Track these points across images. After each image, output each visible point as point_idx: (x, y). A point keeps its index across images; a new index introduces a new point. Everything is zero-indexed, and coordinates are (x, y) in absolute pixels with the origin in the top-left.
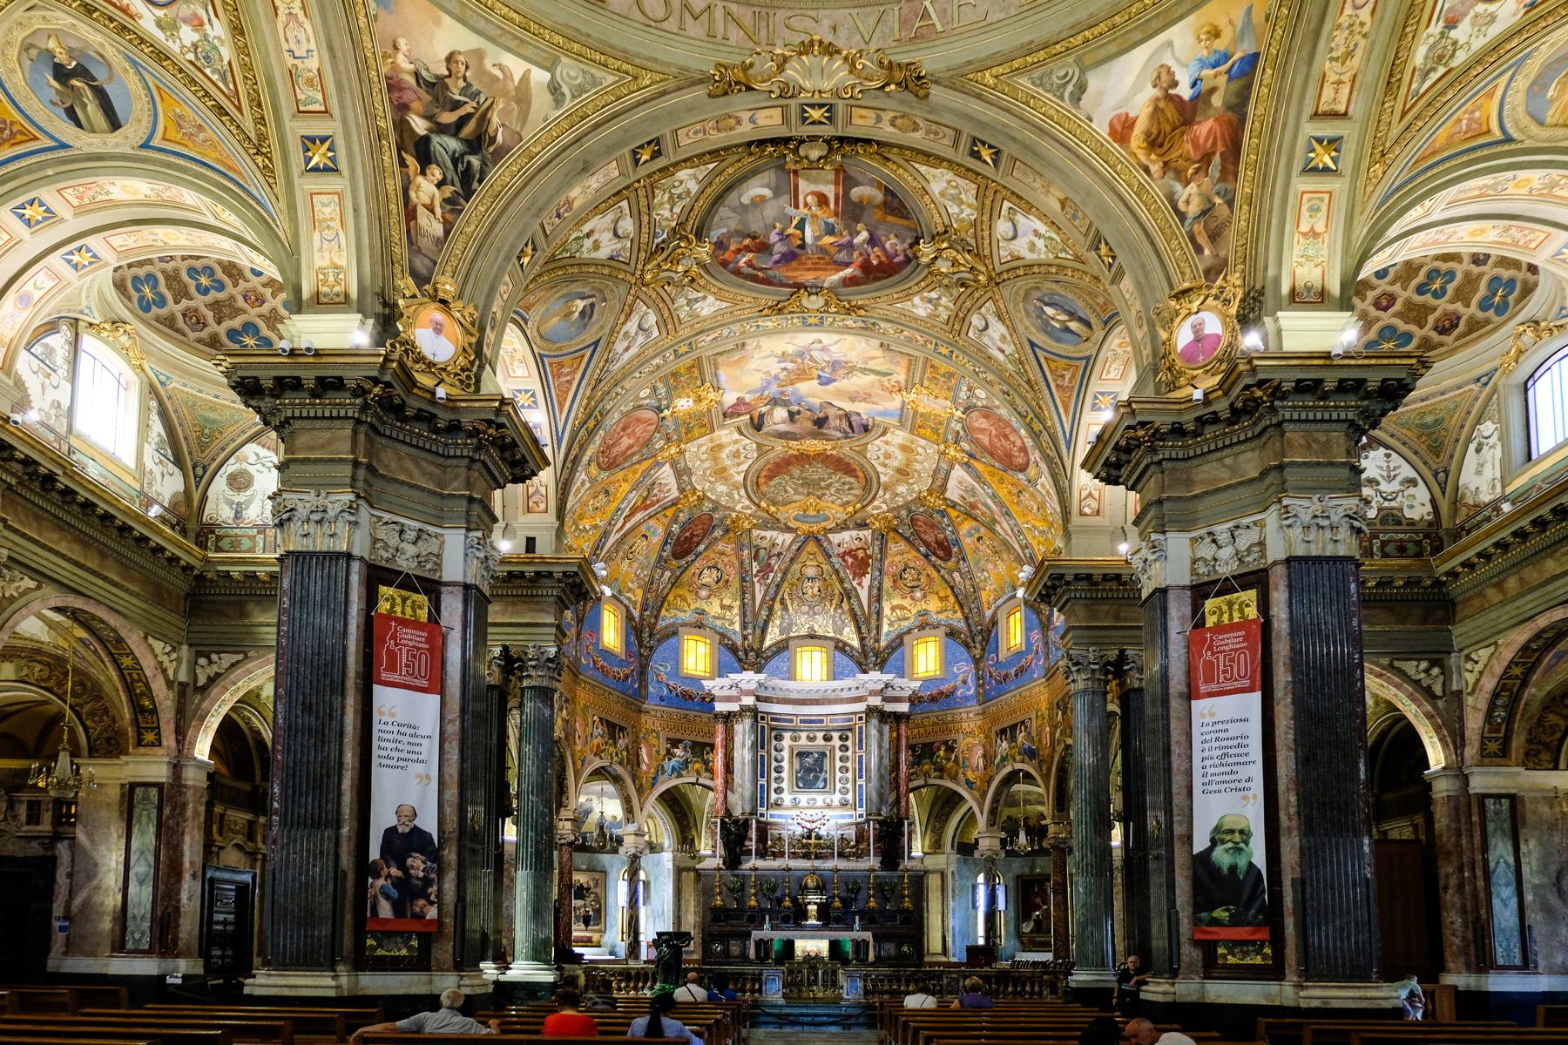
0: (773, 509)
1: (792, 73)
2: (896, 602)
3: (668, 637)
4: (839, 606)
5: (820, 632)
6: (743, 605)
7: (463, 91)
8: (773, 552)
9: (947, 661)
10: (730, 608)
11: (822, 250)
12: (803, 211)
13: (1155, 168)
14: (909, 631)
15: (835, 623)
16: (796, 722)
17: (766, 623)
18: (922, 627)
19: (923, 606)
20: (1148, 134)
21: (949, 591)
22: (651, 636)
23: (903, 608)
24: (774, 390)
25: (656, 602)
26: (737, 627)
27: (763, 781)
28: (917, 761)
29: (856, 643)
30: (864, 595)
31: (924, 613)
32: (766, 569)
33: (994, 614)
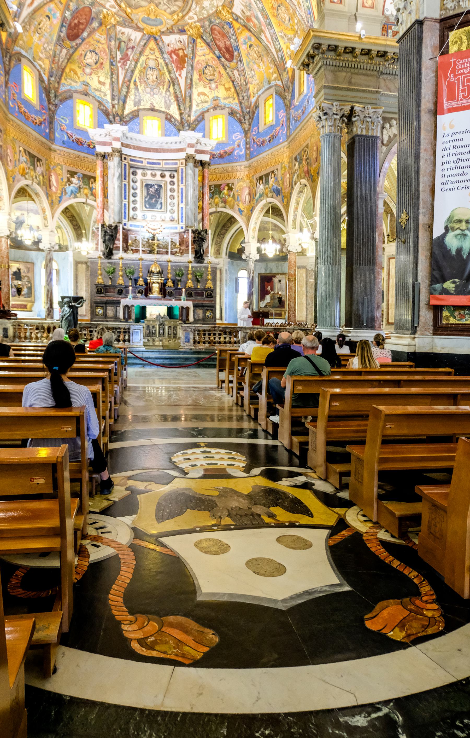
0: (129, 10)
4: (168, 90)
5: (157, 107)
6: (112, 83)
10: (104, 84)
14: (208, 111)
15: (165, 102)
17: (126, 97)
18: (215, 108)
22: (56, 96)
23: (204, 94)
26: (109, 98)
27: (125, 202)
29: (177, 117)
31: (216, 99)
32: (125, 58)
33: (257, 100)
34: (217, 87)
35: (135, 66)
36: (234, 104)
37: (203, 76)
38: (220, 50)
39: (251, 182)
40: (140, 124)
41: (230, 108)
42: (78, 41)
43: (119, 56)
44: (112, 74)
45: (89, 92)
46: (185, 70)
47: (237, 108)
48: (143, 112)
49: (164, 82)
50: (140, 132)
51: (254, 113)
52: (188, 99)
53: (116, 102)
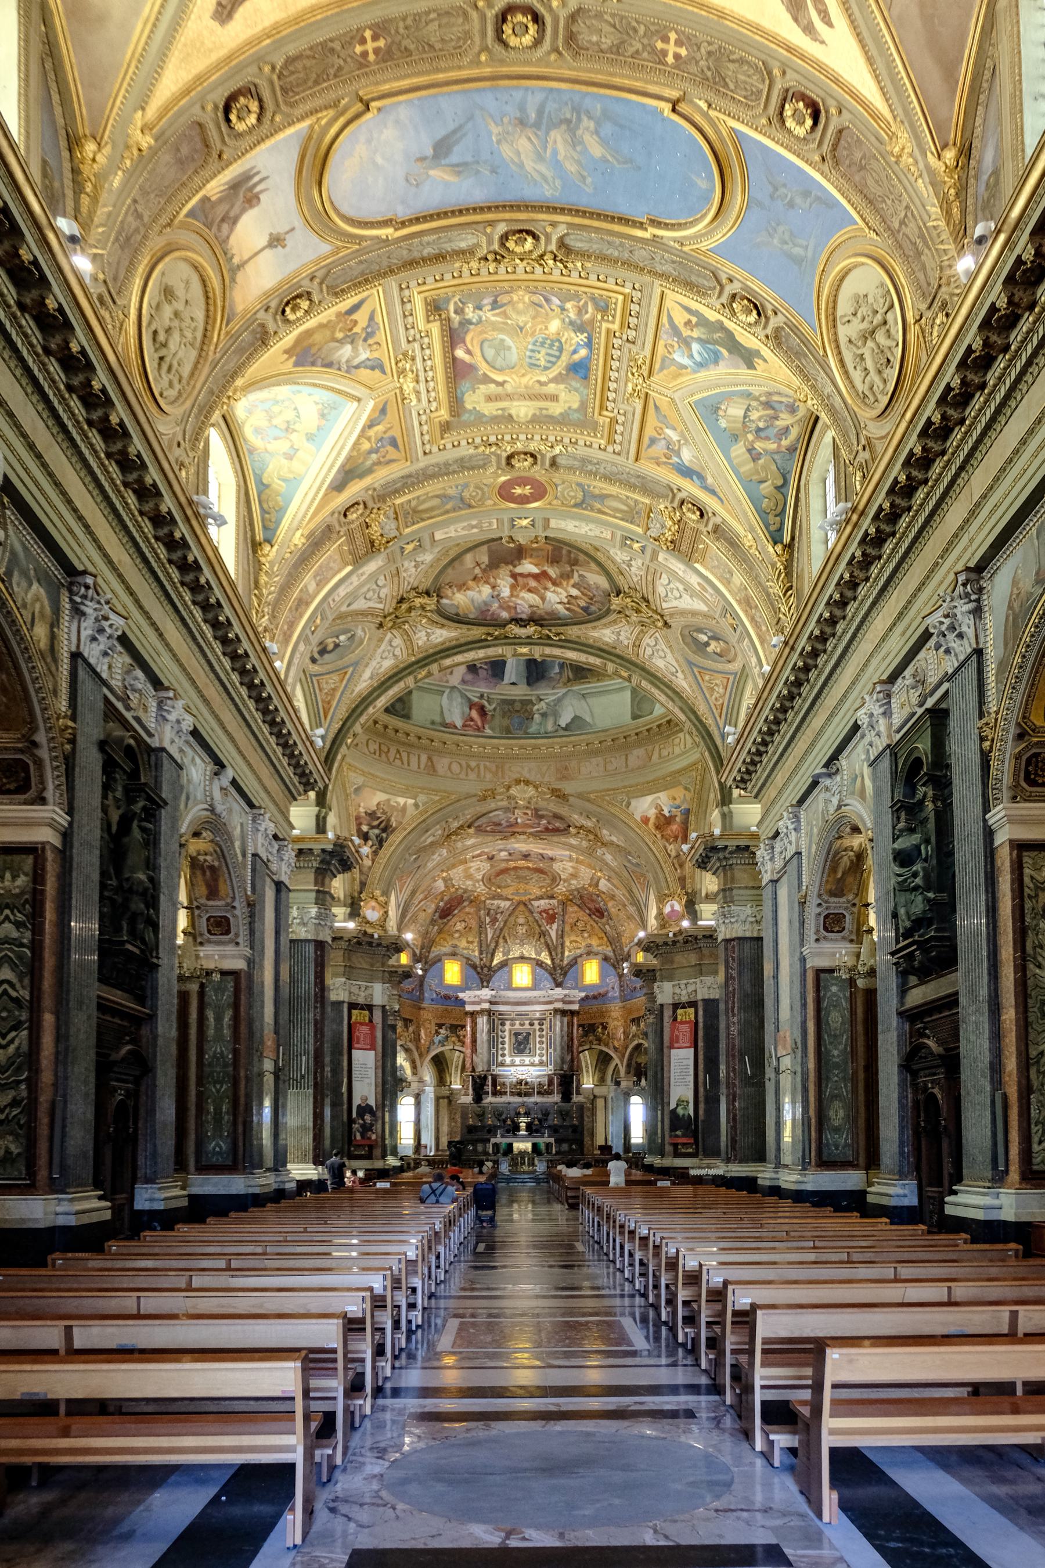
1: (513, 791)
2: (573, 938)
5: (527, 955)
8: (498, 911)
9: (603, 975)
16: (513, 1015)
17: (494, 951)
18: (588, 954)
19: (589, 941)
26: (477, 954)
28: (586, 1034)
29: (549, 962)
30: (553, 934)
31: (589, 946)
32: (494, 920)
40: (510, 973)
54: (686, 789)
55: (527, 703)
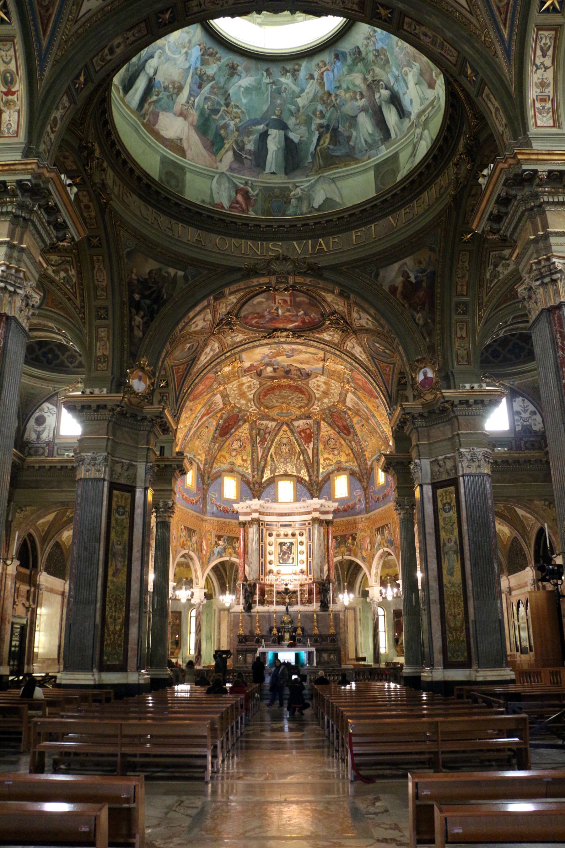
3: (217, 478)
4: (298, 458)
5: (290, 472)
6: (253, 459)
7: (153, 283)
10: (246, 461)
11: (286, 317)
12: (277, 305)
13: (406, 305)
14: (333, 472)
15: (297, 467)
19: (338, 458)
20: (402, 293)
21: (350, 452)
23: (329, 459)
24: (267, 360)
25: (211, 460)
26: (249, 471)
29: (307, 478)
31: (339, 462)
33: (372, 465)
34: (339, 453)
35: (271, 445)
36: (354, 466)
37: (327, 446)
38: (339, 428)
39: (371, 532)
40: (276, 488)
41: (351, 469)
42: (227, 436)
43: (258, 439)
44: (253, 453)
45: (235, 469)
46: (312, 443)
47: (357, 469)
48: (278, 478)
49: (295, 453)
50: (275, 500)
51: (370, 474)
52: (315, 464)
53: (256, 473)
54: (432, 250)
55: (285, 190)
